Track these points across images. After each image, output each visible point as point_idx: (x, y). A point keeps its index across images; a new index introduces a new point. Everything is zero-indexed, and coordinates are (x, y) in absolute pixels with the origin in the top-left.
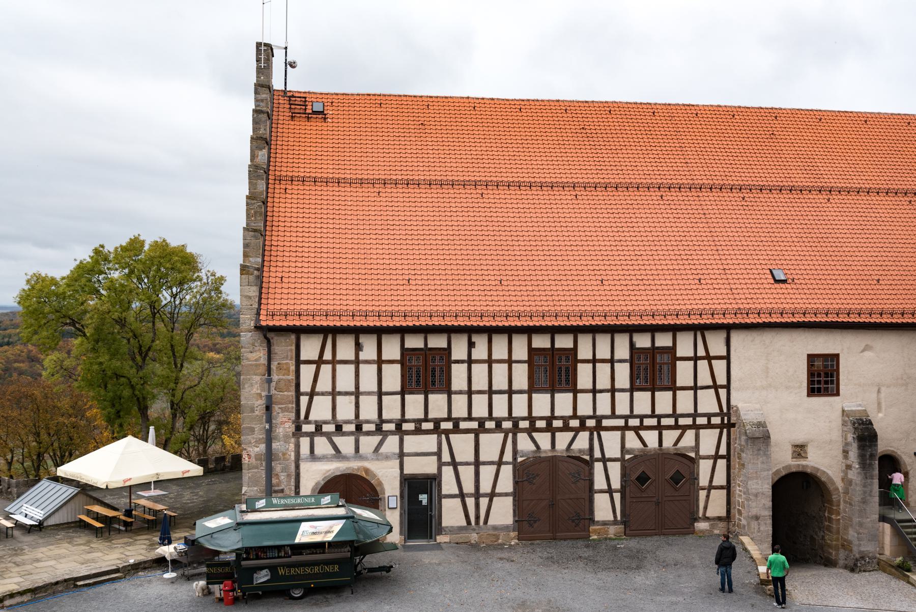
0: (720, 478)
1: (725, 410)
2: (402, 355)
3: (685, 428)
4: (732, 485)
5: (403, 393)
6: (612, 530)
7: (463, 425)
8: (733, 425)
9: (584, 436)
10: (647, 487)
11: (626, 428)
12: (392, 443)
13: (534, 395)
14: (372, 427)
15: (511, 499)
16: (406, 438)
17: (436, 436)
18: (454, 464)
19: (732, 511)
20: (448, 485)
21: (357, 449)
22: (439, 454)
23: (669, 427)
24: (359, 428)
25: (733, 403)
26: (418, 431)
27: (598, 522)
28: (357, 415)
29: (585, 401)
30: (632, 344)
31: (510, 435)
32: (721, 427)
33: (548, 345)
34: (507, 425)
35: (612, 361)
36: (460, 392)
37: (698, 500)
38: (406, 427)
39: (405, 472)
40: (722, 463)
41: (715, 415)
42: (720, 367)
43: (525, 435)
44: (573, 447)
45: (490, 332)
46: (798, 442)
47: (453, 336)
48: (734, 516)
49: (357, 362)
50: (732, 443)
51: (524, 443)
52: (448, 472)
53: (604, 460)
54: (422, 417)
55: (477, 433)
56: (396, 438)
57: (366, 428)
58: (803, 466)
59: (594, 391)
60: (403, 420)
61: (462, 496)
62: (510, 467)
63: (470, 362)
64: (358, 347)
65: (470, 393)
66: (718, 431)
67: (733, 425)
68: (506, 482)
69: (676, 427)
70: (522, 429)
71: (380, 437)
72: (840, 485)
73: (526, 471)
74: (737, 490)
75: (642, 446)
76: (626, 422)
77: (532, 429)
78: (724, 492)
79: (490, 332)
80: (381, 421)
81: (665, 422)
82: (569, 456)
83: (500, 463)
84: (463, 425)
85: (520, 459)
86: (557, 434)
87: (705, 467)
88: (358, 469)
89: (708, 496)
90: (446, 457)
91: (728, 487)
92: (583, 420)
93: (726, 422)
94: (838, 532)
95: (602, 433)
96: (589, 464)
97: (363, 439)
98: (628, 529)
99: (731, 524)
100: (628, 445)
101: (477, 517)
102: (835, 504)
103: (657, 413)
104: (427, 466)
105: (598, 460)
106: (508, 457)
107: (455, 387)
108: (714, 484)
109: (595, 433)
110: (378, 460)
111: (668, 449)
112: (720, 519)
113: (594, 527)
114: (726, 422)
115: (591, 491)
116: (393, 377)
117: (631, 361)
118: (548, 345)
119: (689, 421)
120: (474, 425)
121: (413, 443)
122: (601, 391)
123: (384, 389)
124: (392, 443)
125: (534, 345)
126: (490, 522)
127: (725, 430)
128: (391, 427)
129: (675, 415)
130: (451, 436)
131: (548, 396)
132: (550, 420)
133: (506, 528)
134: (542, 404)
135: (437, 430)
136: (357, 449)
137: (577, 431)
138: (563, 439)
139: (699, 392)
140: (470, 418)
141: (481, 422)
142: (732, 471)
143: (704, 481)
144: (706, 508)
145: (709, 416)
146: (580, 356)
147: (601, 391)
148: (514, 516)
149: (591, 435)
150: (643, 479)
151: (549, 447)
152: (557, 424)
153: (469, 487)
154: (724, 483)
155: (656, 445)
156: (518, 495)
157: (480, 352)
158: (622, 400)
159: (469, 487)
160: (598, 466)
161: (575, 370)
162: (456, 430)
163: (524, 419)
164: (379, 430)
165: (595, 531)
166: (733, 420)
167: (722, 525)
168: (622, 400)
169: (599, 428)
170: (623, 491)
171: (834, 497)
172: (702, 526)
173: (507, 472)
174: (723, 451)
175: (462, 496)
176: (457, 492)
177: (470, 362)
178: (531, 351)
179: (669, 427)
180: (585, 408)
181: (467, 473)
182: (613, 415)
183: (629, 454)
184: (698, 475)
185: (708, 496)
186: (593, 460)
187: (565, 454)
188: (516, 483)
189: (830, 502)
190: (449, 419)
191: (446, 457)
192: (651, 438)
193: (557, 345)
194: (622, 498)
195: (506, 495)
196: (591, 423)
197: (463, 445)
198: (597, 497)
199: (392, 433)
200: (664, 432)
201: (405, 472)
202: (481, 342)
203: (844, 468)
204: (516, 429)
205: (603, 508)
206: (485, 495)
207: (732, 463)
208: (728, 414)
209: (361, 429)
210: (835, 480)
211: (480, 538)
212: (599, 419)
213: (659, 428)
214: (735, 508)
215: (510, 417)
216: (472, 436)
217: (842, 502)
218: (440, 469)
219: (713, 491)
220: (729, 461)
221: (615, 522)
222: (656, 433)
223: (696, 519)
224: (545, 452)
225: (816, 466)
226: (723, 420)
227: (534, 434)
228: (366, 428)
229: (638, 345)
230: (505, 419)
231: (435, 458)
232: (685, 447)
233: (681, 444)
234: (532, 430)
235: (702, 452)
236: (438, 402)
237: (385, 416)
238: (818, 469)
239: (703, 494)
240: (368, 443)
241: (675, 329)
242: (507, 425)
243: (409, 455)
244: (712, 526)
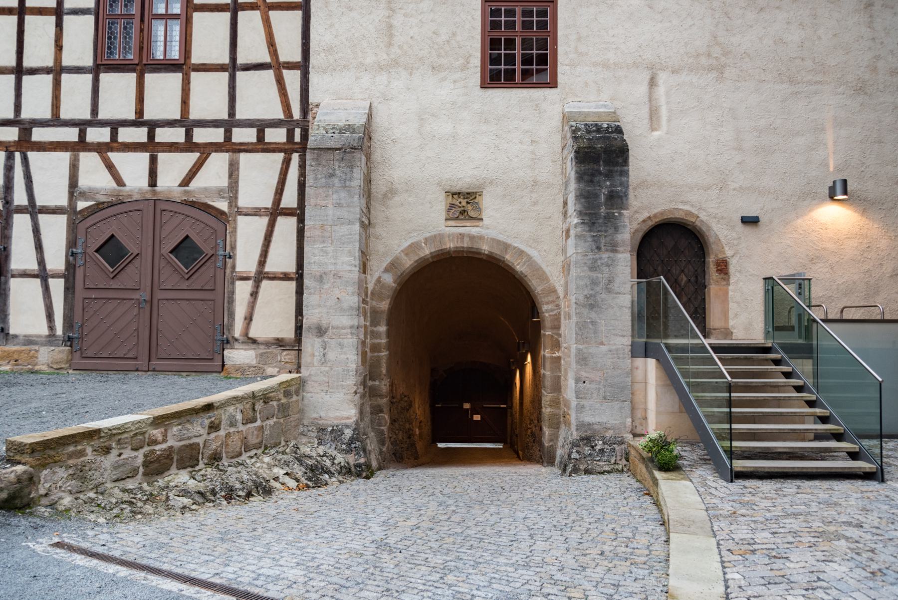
1: (297, 114)
11: (82, 145)
23: (173, 147)
32: (287, 149)
53: (33, 210)
66: (280, 156)
69: (189, 145)
76: (82, 134)
78: (292, 285)
81: (163, 135)
89: (254, 294)
93: (297, 138)
95: (31, 155)
100: (84, 182)
103: (146, 117)
105: (20, 210)
109: (17, 155)
111: (170, 190)
112: (280, 343)
119: (216, 135)
122: (33, 71)
127: (295, 157)
129: (186, 123)
144: (249, 319)
145: (261, 126)
147: (33, 71)
149: (10, 157)
170: (69, 275)
172: (238, 356)
174: (290, 199)
179: (173, 147)
182: (56, 121)
183: (86, 200)
185: (254, 294)
200: (161, 156)
213: (151, 147)
219: (265, 284)
222: (145, 157)
223: (227, 342)
226: (290, 134)
232: (206, 190)
235: (244, 201)
239: (243, 290)
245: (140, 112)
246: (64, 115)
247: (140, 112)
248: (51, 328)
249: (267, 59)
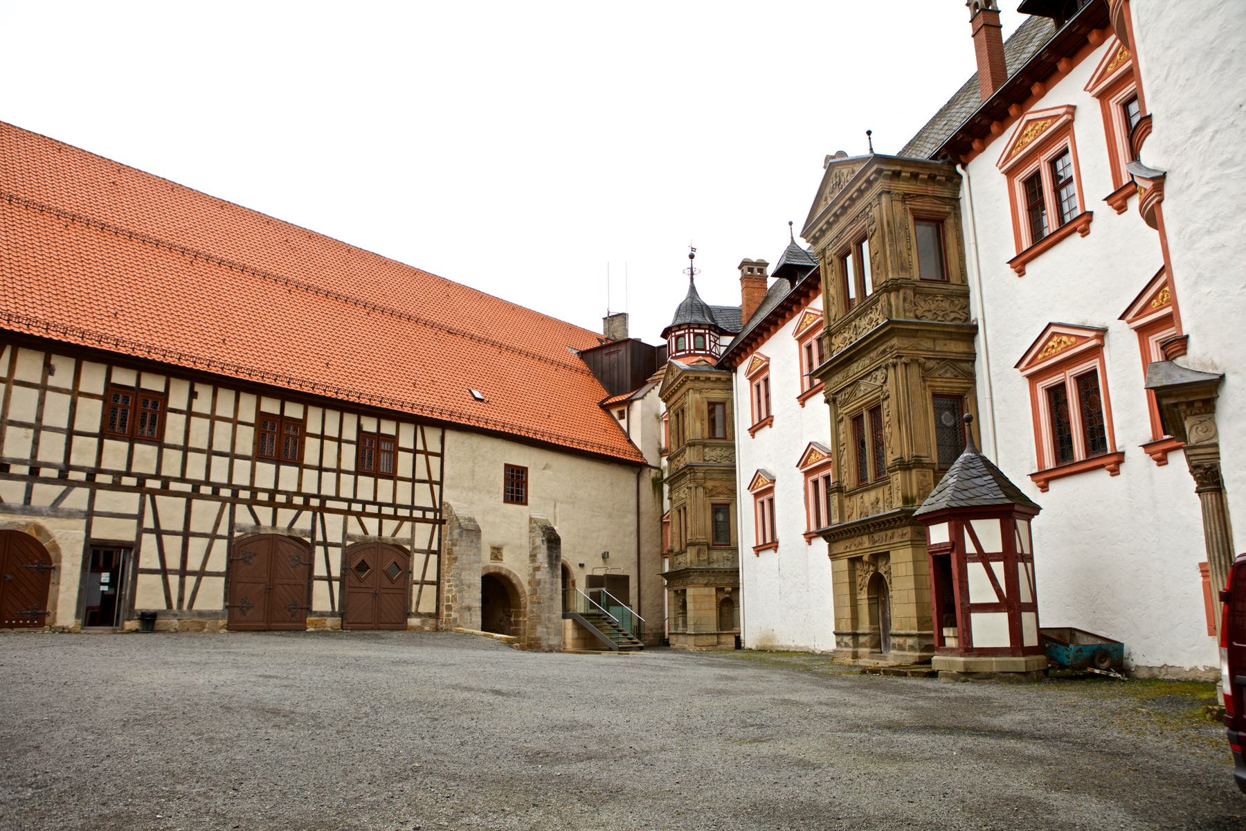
0: (431, 575)
1: (438, 507)
2: (106, 389)
3: (403, 519)
4: (442, 581)
5: (102, 436)
6: (330, 622)
7: (174, 486)
8: (444, 522)
9: (307, 516)
10: (366, 577)
11: (349, 512)
12: (78, 499)
13: (258, 464)
14: (54, 473)
15: (222, 580)
16: (99, 493)
17: (138, 495)
18: (158, 532)
19: (441, 608)
20: (148, 556)
21: (28, 499)
22: (140, 517)
23: (389, 517)
24: (34, 471)
25: (444, 499)
26: (116, 486)
27: (316, 612)
28: (34, 455)
29: (310, 477)
30: (359, 427)
31: (228, 505)
32: (434, 522)
33: (278, 412)
34: (226, 493)
35: (339, 440)
36: (174, 447)
37: (411, 595)
38: (100, 478)
39: (93, 536)
40: (433, 558)
41: (429, 510)
42: (435, 462)
43: (245, 507)
44: (295, 527)
45: (218, 382)
46: (496, 545)
47: (173, 382)
48: (442, 613)
49: (43, 388)
50: (443, 539)
51: (243, 516)
52: (149, 541)
53: (326, 544)
54: (124, 469)
55: (189, 498)
56: (84, 492)
57: (44, 472)
58: (499, 568)
59: (321, 469)
60: (98, 470)
61: (164, 572)
62: (225, 542)
63: (189, 413)
64: (48, 369)
65: (186, 449)
66: (431, 525)
67: (444, 522)
68: (218, 561)
69: (395, 517)
70: (241, 499)
71: (64, 488)
72: (527, 588)
73: (242, 549)
74: (446, 586)
75: (363, 533)
76: (350, 507)
77: (252, 502)
78: (435, 587)
79: (218, 382)
80: (66, 467)
82: (290, 537)
83: (213, 536)
84: (174, 486)
85: (236, 534)
86: (280, 510)
87: (418, 560)
88: (27, 525)
89: (420, 591)
90: (149, 522)
91: (438, 583)
92: (307, 497)
93: (438, 518)
94: (525, 634)
95: (326, 515)
96: (310, 548)
97: (38, 487)
98: (345, 622)
99: (439, 621)
100: (350, 531)
101: (181, 600)
102: (522, 606)
103: (378, 500)
104: (124, 532)
105: (319, 544)
106: (223, 530)
107: (168, 439)
108: (426, 579)
109: (318, 514)
110: (56, 516)
111: (387, 539)
112: (429, 615)
113: (311, 619)
114: (438, 518)
115: (310, 577)
116: (91, 415)
117: (358, 443)
118: (278, 412)
119: (406, 513)
120: (187, 488)
121: (106, 499)
122: (327, 470)
123: (77, 427)
124: (78, 499)
125: (263, 409)
126: (196, 607)
127: (437, 526)
128: (82, 476)
129: (395, 505)
130: (158, 498)
131: (274, 466)
132: (273, 493)
133: (213, 615)
134: (265, 474)
135: (140, 488)
136: (28, 499)
137: (300, 509)
138: (285, 516)
139: (416, 484)
140: (182, 479)
141: (196, 485)
142: (442, 567)
143: (417, 576)
144: (418, 603)
145: (424, 510)
146: (309, 429)
147: (327, 470)
148: (225, 600)
150: (363, 567)
151: (269, 523)
152: (281, 498)
153: (173, 562)
154: (434, 579)
155: (376, 534)
156: (230, 575)
157: (202, 404)
158: (347, 480)
159: (173, 562)
160: (319, 551)
161: (303, 443)
162: (165, 490)
163: (244, 488)
164: (63, 478)
165: (312, 622)
166: (445, 516)
167: (432, 621)
168: (347, 480)
169: (323, 509)
170: (342, 580)
171: (522, 599)
172: (414, 621)
173: (221, 547)
174: (435, 547)
175: (164, 572)
176: (158, 566)
177: (189, 413)
178: (260, 415)
179: (389, 517)
180: (310, 486)
181: (173, 545)
182: (337, 498)
183: (351, 540)
184: (412, 568)
185: (420, 591)
186: (315, 543)
187: (286, 534)
188: (230, 562)
189: (518, 606)
190: (157, 476)
191: (149, 522)
192: (372, 524)
193: (287, 414)
194: (340, 587)
195: (218, 574)
196: (315, 502)
197: (171, 511)
198: (316, 584)
199: (79, 484)
200: (384, 521)
201: (93, 536)
202: (204, 392)
203: (531, 571)
204: (235, 500)
205: (322, 598)
206: (193, 573)
207: (442, 560)
208: (440, 511)
209: (38, 473)
210: (523, 583)
211: (181, 625)
212: (324, 499)
213: (380, 516)
214: (443, 605)
215: (229, 485)
216: (183, 500)
217: (528, 603)
218: (139, 537)
219: (425, 586)
220: (439, 557)
221: (333, 614)
222: (377, 521)
223: (409, 615)
224: (265, 528)
225: (509, 568)
226: (435, 515)
227: (255, 507)
228: (44, 472)
229: (365, 429)
230: (223, 486)
231: (135, 522)
232: (402, 539)
233: (399, 536)
234: (252, 502)
235: (417, 546)
236: (145, 456)
237: (74, 461)
238: (510, 572)
239: (416, 588)
240: (44, 494)
241: (399, 417)
242: (226, 493)
243: (101, 514)
244: (423, 622)
245: (375, 497)
246: (342, 495)
247: (375, 497)
248: (333, 607)
249: (427, 478)
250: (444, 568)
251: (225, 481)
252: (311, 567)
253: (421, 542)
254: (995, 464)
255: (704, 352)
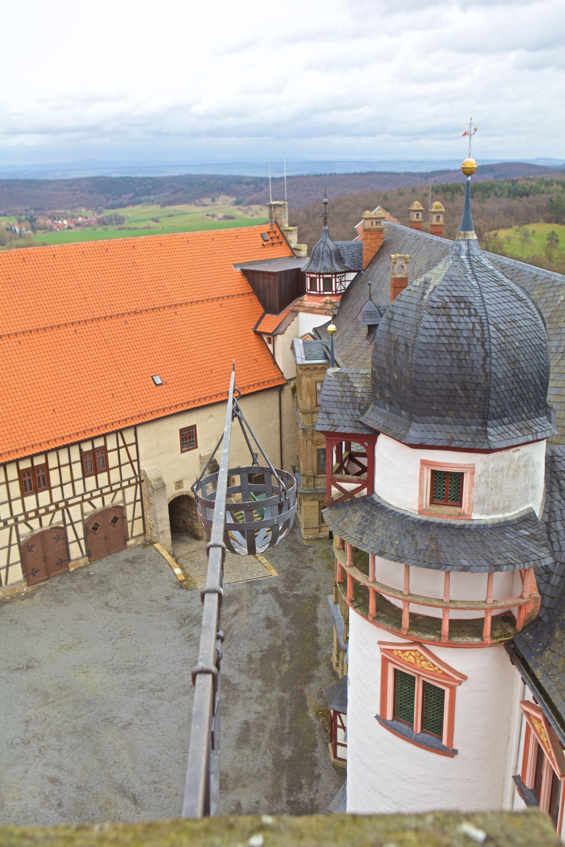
0: (138, 513)
1: (137, 473)
25: (141, 468)
40: (138, 504)
42: (132, 449)
89: (133, 525)
91: (143, 517)
96: (64, 529)
106: (14, 540)
115: (67, 544)
143: (129, 517)
144: (132, 532)
155: (101, 505)
166: (142, 478)
170: (85, 538)
174: (138, 497)
185: (133, 525)
208: (140, 476)
223: (128, 540)
239: (130, 525)
244: (137, 541)
250: (145, 507)
251: (9, 516)
252: (66, 538)
253: (130, 498)
254: (527, 687)
255: (330, 293)
